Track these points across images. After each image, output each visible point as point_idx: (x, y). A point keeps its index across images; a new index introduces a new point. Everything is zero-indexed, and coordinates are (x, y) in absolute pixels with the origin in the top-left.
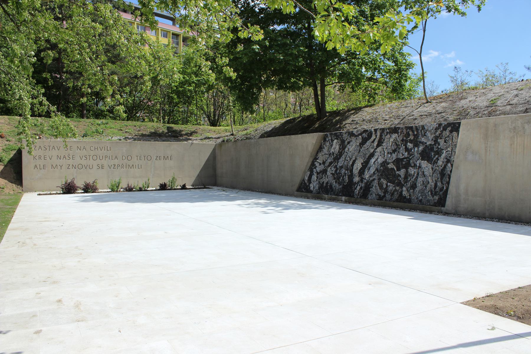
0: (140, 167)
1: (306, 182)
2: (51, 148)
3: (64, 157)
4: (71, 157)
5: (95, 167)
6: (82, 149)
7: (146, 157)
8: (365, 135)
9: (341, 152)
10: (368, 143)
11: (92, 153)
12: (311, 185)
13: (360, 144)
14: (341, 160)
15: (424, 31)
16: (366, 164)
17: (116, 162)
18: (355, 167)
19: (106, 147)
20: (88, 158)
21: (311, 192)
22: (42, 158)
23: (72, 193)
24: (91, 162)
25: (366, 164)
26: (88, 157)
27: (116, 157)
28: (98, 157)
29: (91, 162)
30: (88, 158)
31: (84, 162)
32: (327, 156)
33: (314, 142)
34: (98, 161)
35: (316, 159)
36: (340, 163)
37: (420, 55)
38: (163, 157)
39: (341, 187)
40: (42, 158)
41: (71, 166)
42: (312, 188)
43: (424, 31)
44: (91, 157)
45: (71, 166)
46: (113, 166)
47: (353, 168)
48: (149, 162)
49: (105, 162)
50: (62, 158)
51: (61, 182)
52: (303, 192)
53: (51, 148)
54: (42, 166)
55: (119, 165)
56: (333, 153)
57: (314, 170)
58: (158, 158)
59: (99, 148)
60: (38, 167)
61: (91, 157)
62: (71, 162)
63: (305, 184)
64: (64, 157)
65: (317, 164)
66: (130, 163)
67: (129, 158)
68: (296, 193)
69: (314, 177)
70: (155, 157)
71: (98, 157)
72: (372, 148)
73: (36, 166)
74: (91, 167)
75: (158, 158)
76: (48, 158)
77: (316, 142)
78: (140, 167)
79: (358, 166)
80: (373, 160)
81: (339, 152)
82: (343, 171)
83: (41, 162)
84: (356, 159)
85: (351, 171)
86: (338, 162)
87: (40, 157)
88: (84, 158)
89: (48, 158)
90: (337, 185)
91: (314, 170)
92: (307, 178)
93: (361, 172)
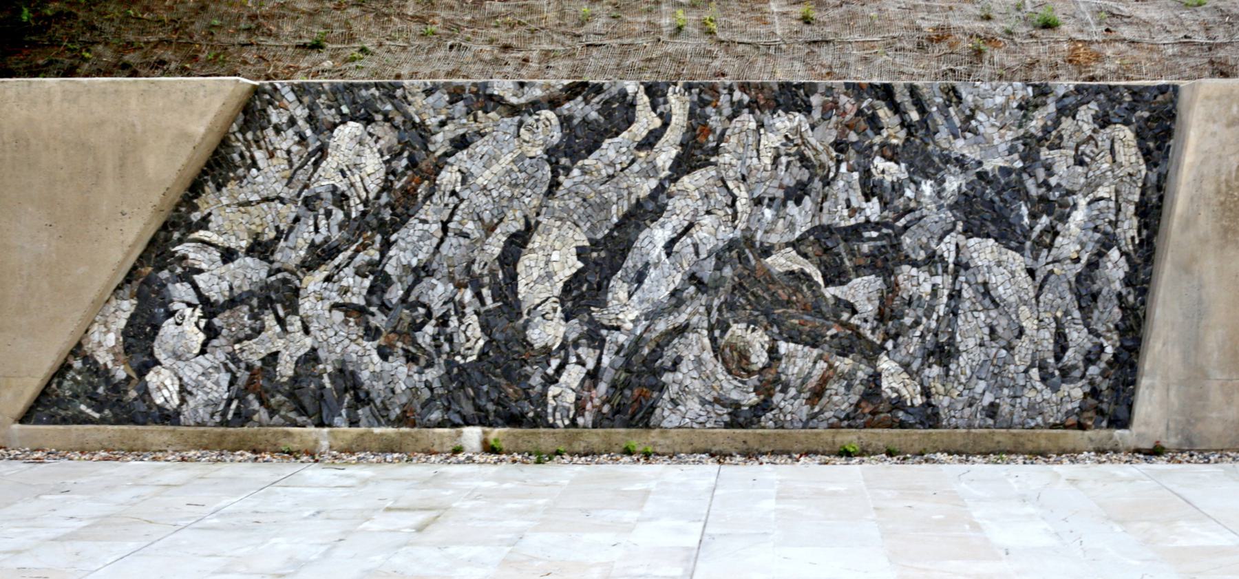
9: (409, 193)
14: (413, 229)
16: (607, 258)
18: (529, 266)
25: (607, 258)
32: (290, 211)
36: (411, 245)
39: (431, 374)
47: (513, 278)
56: (341, 199)
80: (659, 234)
81: (386, 187)
82: (437, 292)
84: (530, 228)
85: (507, 289)
86: (387, 245)
90: (399, 369)
93: (582, 295)
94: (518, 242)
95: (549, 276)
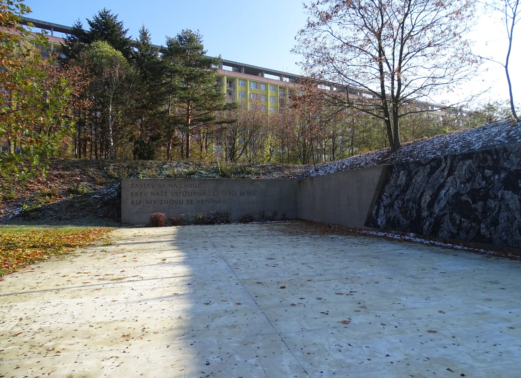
1: (374, 216)
2: (146, 186)
3: (158, 193)
4: (164, 193)
8: (433, 164)
9: (408, 184)
10: (437, 173)
12: (379, 220)
13: (428, 174)
15: (511, 39)
16: (435, 197)
17: (204, 197)
18: (423, 201)
20: (179, 195)
21: (379, 227)
22: (139, 194)
25: (435, 197)
27: (204, 194)
30: (179, 195)
33: (380, 174)
35: (382, 192)
37: (506, 67)
39: (409, 221)
40: (139, 194)
41: (163, 201)
42: (379, 223)
43: (511, 39)
44: (181, 193)
45: (163, 201)
46: (201, 201)
50: (156, 194)
52: (370, 226)
53: (146, 186)
54: (138, 201)
55: (206, 201)
56: (400, 186)
57: (382, 203)
60: (135, 202)
61: (181, 193)
63: (373, 218)
64: (158, 193)
65: (384, 198)
67: (216, 194)
68: (364, 227)
69: (382, 211)
72: (442, 178)
73: (133, 202)
77: (381, 174)
79: (427, 198)
80: (443, 192)
81: (406, 183)
82: (411, 204)
85: (419, 204)
86: (405, 195)
88: (175, 194)
89: (144, 195)
91: (382, 203)
92: (374, 212)
93: (430, 206)
94: (422, 194)
95: (426, 201)
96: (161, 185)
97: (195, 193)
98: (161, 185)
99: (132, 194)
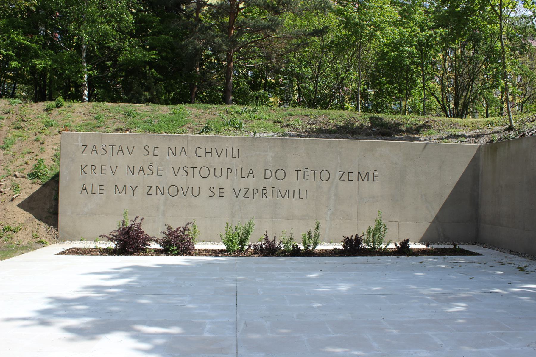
0: (303, 195)
2: (116, 149)
3: (142, 169)
4: (155, 169)
5: (205, 192)
6: (178, 152)
7: (317, 174)
11: (200, 162)
17: (250, 182)
19: (229, 150)
20: (190, 174)
22: (98, 170)
23: (132, 254)
24: (196, 182)
26: (190, 171)
27: (251, 172)
28: (212, 170)
29: (196, 182)
30: (190, 174)
31: (181, 181)
34: (212, 181)
38: (355, 174)
40: (98, 170)
41: (154, 188)
44: (197, 171)
45: (154, 188)
46: (243, 192)
48: (325, 186)
49: (225, 182)
51: (112, 225)
53: (116, 149)
54: (96, 187)
55: (256, 191)
58: (345, 177)
59: (214, 151)
60: (89, 190)
61: (197, 171)
62: (154, 180)
64: (142, 169)
66: (282, 186)
67: (280, 174)
70: (339, 174)
71: (212, 170)
73: (84, 188)
74: (196, 193)
75: (345, 177)
76: (109, 172)
78: (303, 195)
83: (95, 180)
87: (93, 169)
88: (182, 173)
89: (109, 172)
96: (151, 149)
97: (229, 171)
98: (151, 149)
99: (82, 169)
